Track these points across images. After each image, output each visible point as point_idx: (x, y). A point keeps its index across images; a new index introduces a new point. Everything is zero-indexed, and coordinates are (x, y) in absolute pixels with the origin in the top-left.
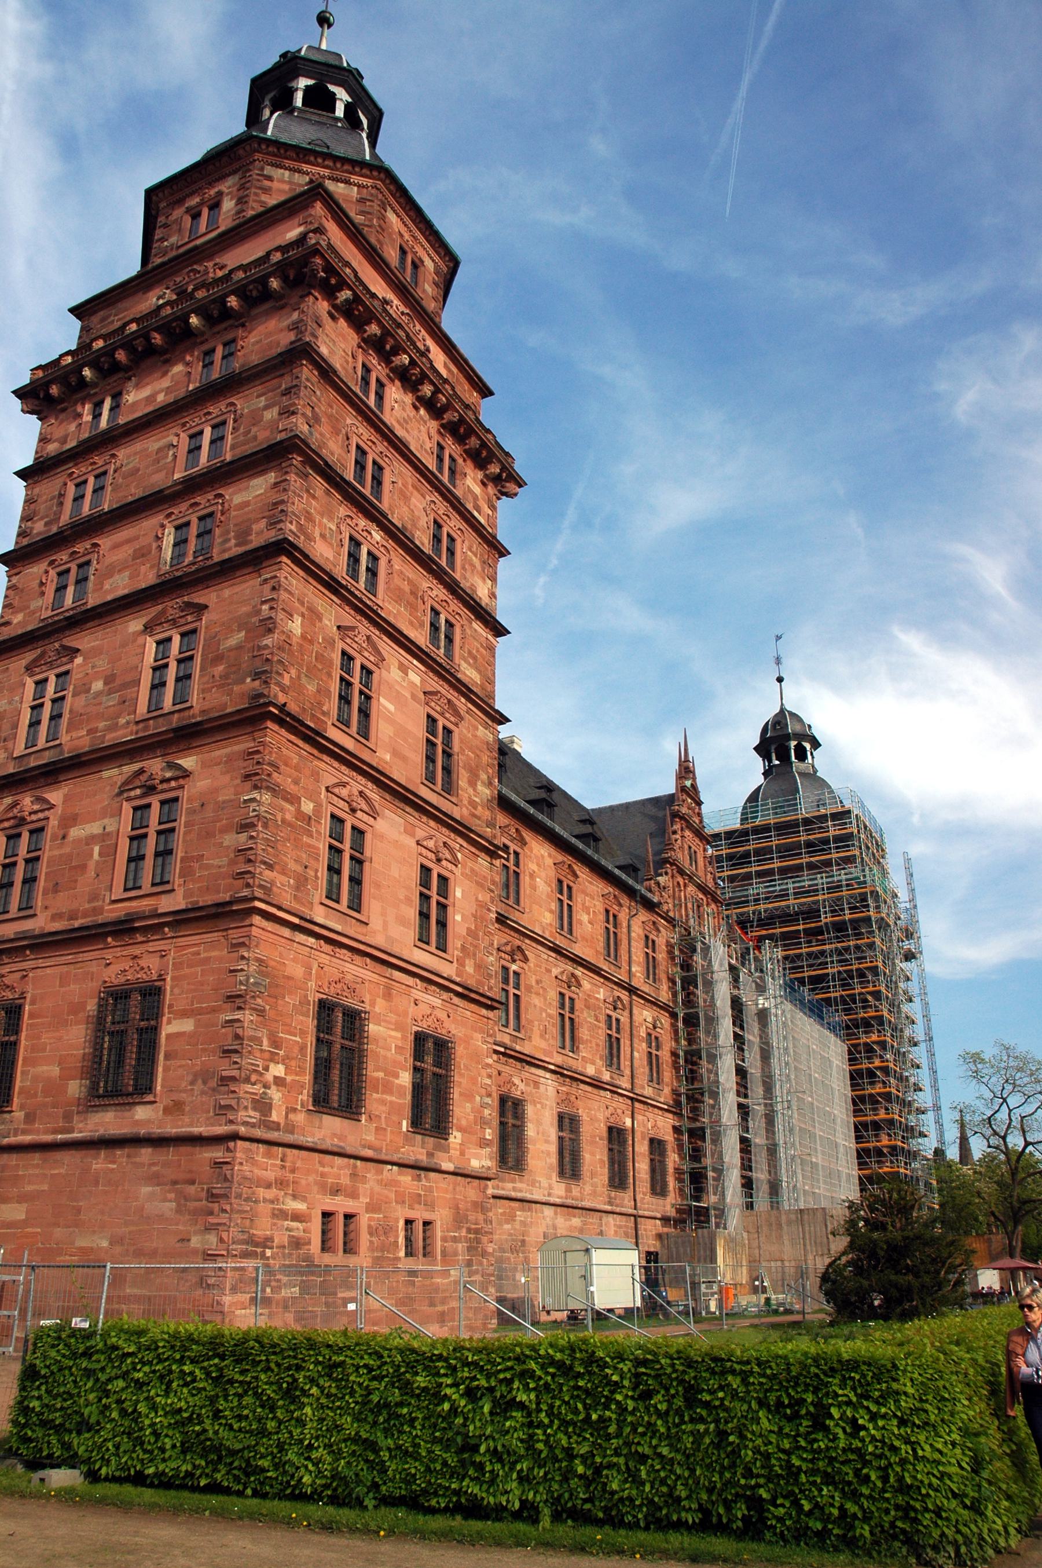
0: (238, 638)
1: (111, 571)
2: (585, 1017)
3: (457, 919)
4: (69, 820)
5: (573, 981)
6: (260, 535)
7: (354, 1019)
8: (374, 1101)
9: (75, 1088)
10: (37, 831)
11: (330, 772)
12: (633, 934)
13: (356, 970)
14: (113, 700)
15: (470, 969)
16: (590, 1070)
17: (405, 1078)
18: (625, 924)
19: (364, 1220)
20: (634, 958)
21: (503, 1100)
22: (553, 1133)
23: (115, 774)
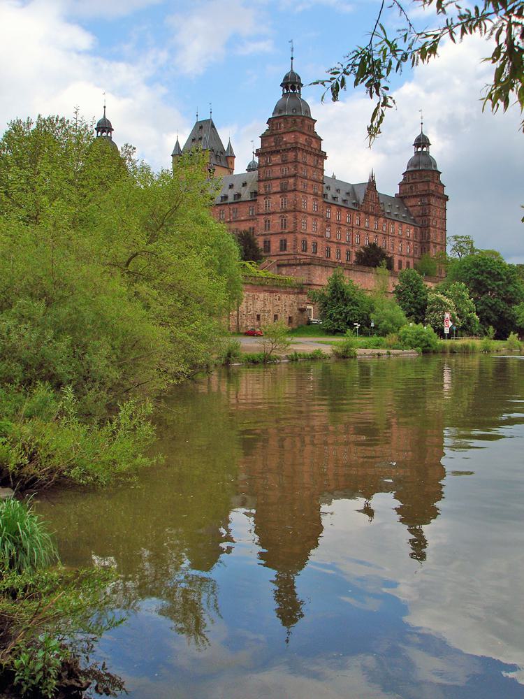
5: (340, 228)
6: (293, 188)
10: (269, 221)
11: (302, 215)
13: (306, 236)
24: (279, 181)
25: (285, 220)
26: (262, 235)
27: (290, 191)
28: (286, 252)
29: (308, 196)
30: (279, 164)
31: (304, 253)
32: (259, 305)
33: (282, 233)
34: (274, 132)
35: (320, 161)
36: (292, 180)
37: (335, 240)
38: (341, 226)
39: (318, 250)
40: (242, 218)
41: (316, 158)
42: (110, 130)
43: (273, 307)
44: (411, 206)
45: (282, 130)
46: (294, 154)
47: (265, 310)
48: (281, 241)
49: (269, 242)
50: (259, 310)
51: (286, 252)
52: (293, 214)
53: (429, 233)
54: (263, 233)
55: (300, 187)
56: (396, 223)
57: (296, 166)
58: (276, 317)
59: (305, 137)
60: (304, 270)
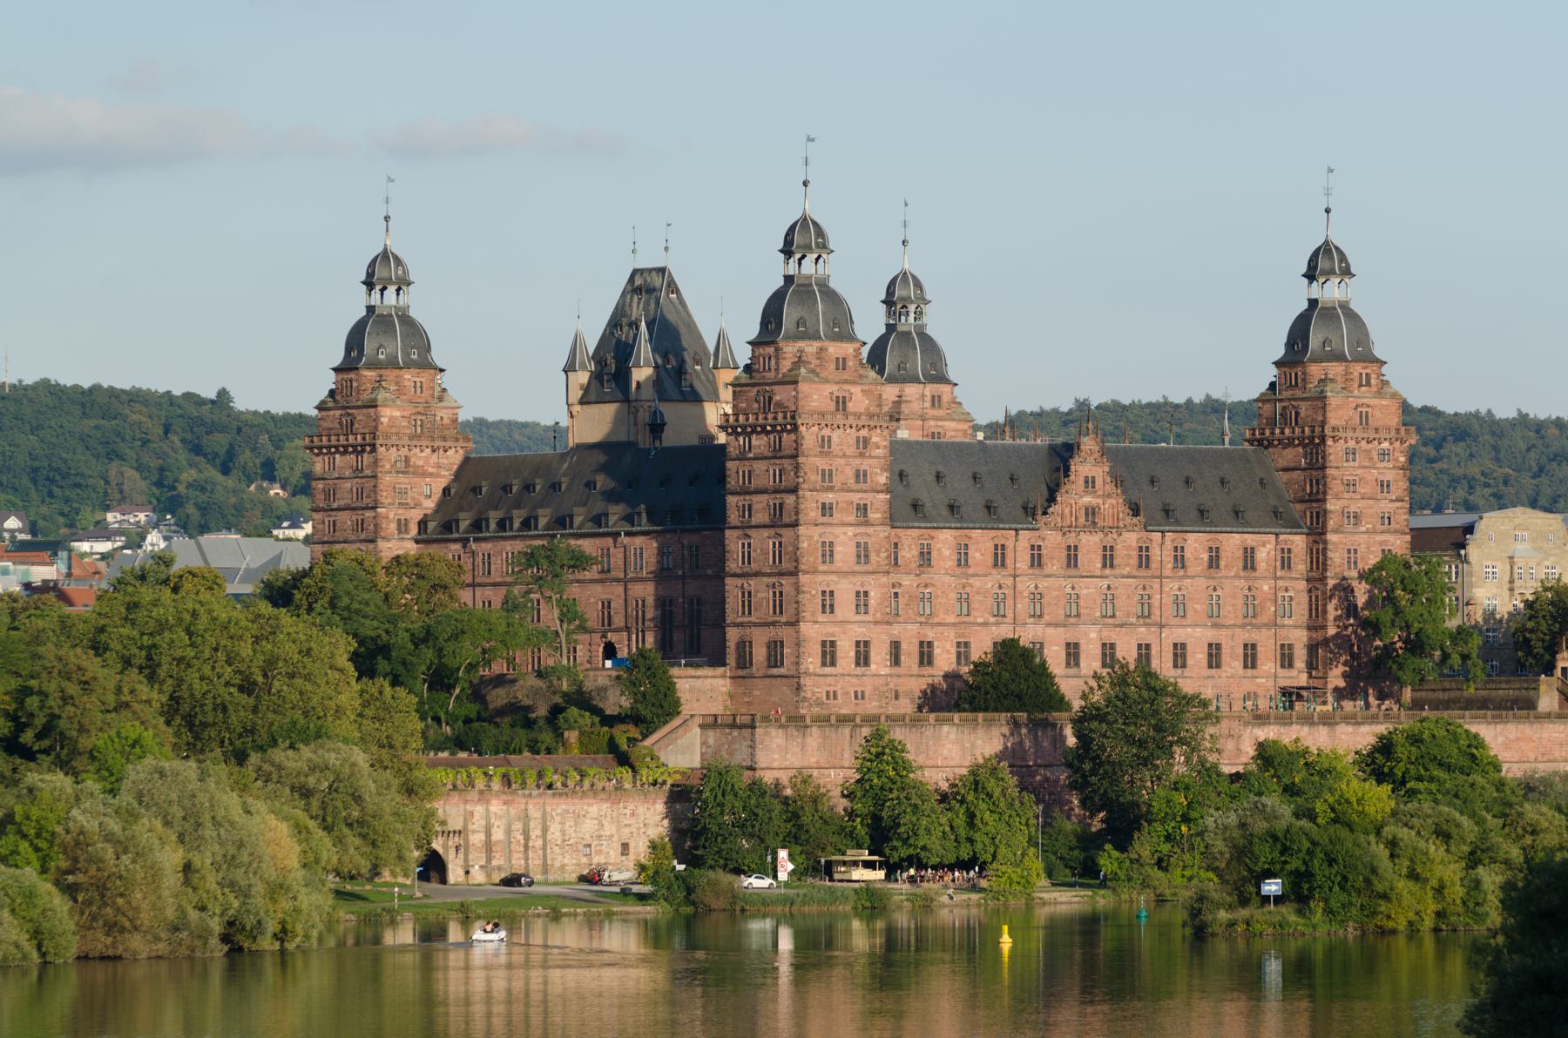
0: (790, 549)
1: (757, 512)
2: (976, 600)
3: (872, 602)
4: (757, 591)
7: (833, 643)
8: (840, 662)
9: (765, 664)
11: (820, 578)
12: (1018, 549)
13: (832, 629)
14: (763, 557)
15: (878, 615)
16: (980, 620)
17: (853, 654)
18: (1011, 546)
19: (839, 693)
20: (1019, 559)
21: (921, 643)
22: (954, 650)
23: (766, 580)
24: (765, 497)
25: (781, 593)
26: (741, 625)
27: (787, 526)
28: (782, 671)
29: (838, 530)
30: (766, 458)
31: (828, 670)
32: (588, 826)
33: (773, 624)
34: (758, 375)
35: (875, 439)
36: (790, 500)
37: (951, 619)
38: (971, 581)
39: (873, 656)
40: (709, 572)
41: (864, 432)
42: (403, 283)
43: (618, 830)
44: (1285, 470)
45: (771, 375)
46: (793, 436)
47: (600, 836)
48: (775, 642)
49: (751, 643)
50: (587, 836)
51: (782, 671)
52: (792, 579)
53: (1325, 549)
54: (739, 620)
55: (812, 514)
56: (1191, 537)
57: (797, 467)
58: (625, 846)
59: (829, 388)
60: (744, 738)
